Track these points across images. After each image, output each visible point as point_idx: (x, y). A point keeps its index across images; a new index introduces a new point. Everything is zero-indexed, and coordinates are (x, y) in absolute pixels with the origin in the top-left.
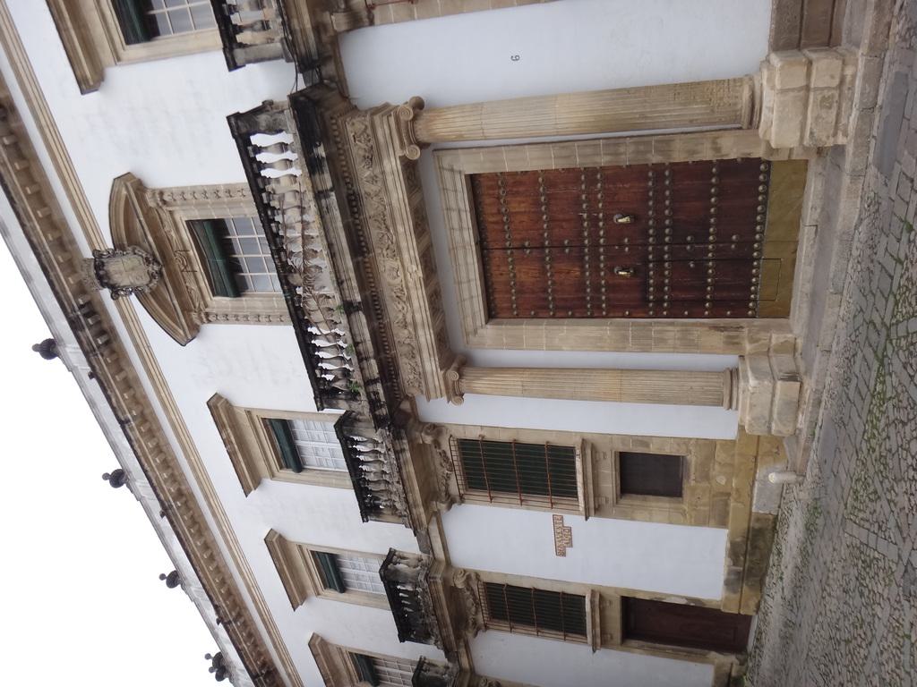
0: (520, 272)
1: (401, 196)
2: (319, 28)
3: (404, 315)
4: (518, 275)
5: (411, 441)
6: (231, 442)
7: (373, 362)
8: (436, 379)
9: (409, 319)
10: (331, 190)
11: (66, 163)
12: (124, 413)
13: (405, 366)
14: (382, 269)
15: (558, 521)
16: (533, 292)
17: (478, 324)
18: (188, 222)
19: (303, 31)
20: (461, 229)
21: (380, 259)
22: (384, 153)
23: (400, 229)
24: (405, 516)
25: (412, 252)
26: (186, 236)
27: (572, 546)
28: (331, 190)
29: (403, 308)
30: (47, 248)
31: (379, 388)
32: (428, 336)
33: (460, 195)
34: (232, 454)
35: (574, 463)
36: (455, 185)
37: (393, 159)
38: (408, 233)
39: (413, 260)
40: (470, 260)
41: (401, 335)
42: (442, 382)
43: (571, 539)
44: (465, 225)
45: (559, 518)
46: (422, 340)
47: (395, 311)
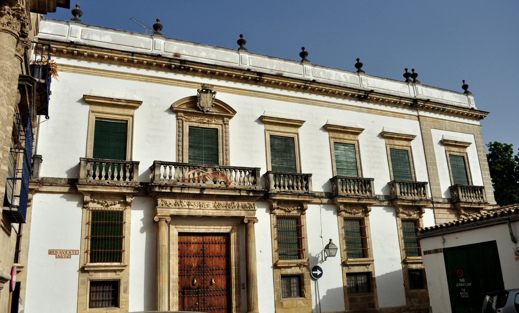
0: (195, 246)
1: (233, 214)
2: (275, 200)
3: (193, 205)
4: (193, 245)
5: (129, 193)
6: (118, 101)
7: (179, 191)
8: (167, 212)
9: (190, 207)
10: (240, 194)
11: (238, 93)
12: (137, 56)
13: (172, 201)
14: (210, 201)
15: (75, 252)
16: (187, 250)
17: (179, 229)
18: (217, 129)
19: (276, 196)
20: (214, 229)
21: (214, 202)
22: (246, 212)
23: (224, 211)
24: (87, 181)
25: (216, 213)
26: (213, 126)
27: (56, 258)
28: (240, 194)
29: (195, 206)
30: (214, 70)
31: (168, 190)
32: (185, 213)
33: (225, 230)
34: (111, 99)
35: (116, 262)
36: (228, 229)
37: (244, 214)
38: (222, 214)
39: (213, 213)
40: (203, 230)
41: (185, 202)
42: (164, 214)
43: (62, 257)
44: (215, 230)
45: (77, 252)
46: (183, 210)
47: (195, 203)
